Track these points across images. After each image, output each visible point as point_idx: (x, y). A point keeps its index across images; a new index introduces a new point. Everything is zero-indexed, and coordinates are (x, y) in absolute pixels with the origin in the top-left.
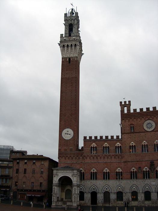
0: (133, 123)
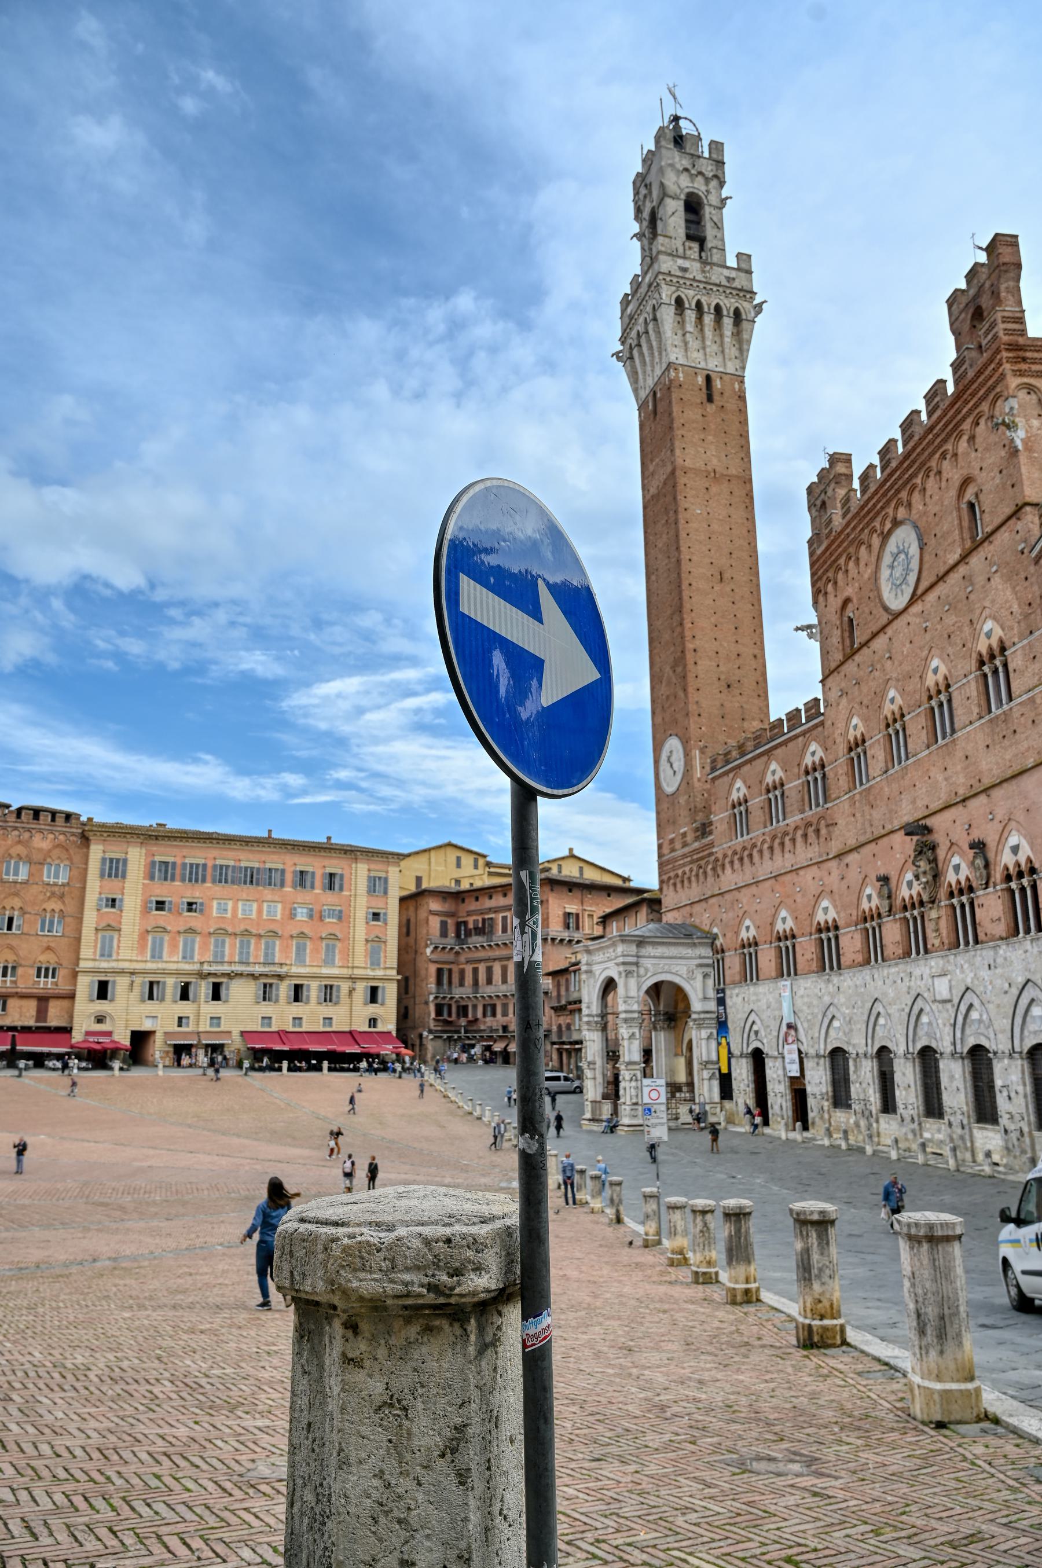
0: (849, 591)
